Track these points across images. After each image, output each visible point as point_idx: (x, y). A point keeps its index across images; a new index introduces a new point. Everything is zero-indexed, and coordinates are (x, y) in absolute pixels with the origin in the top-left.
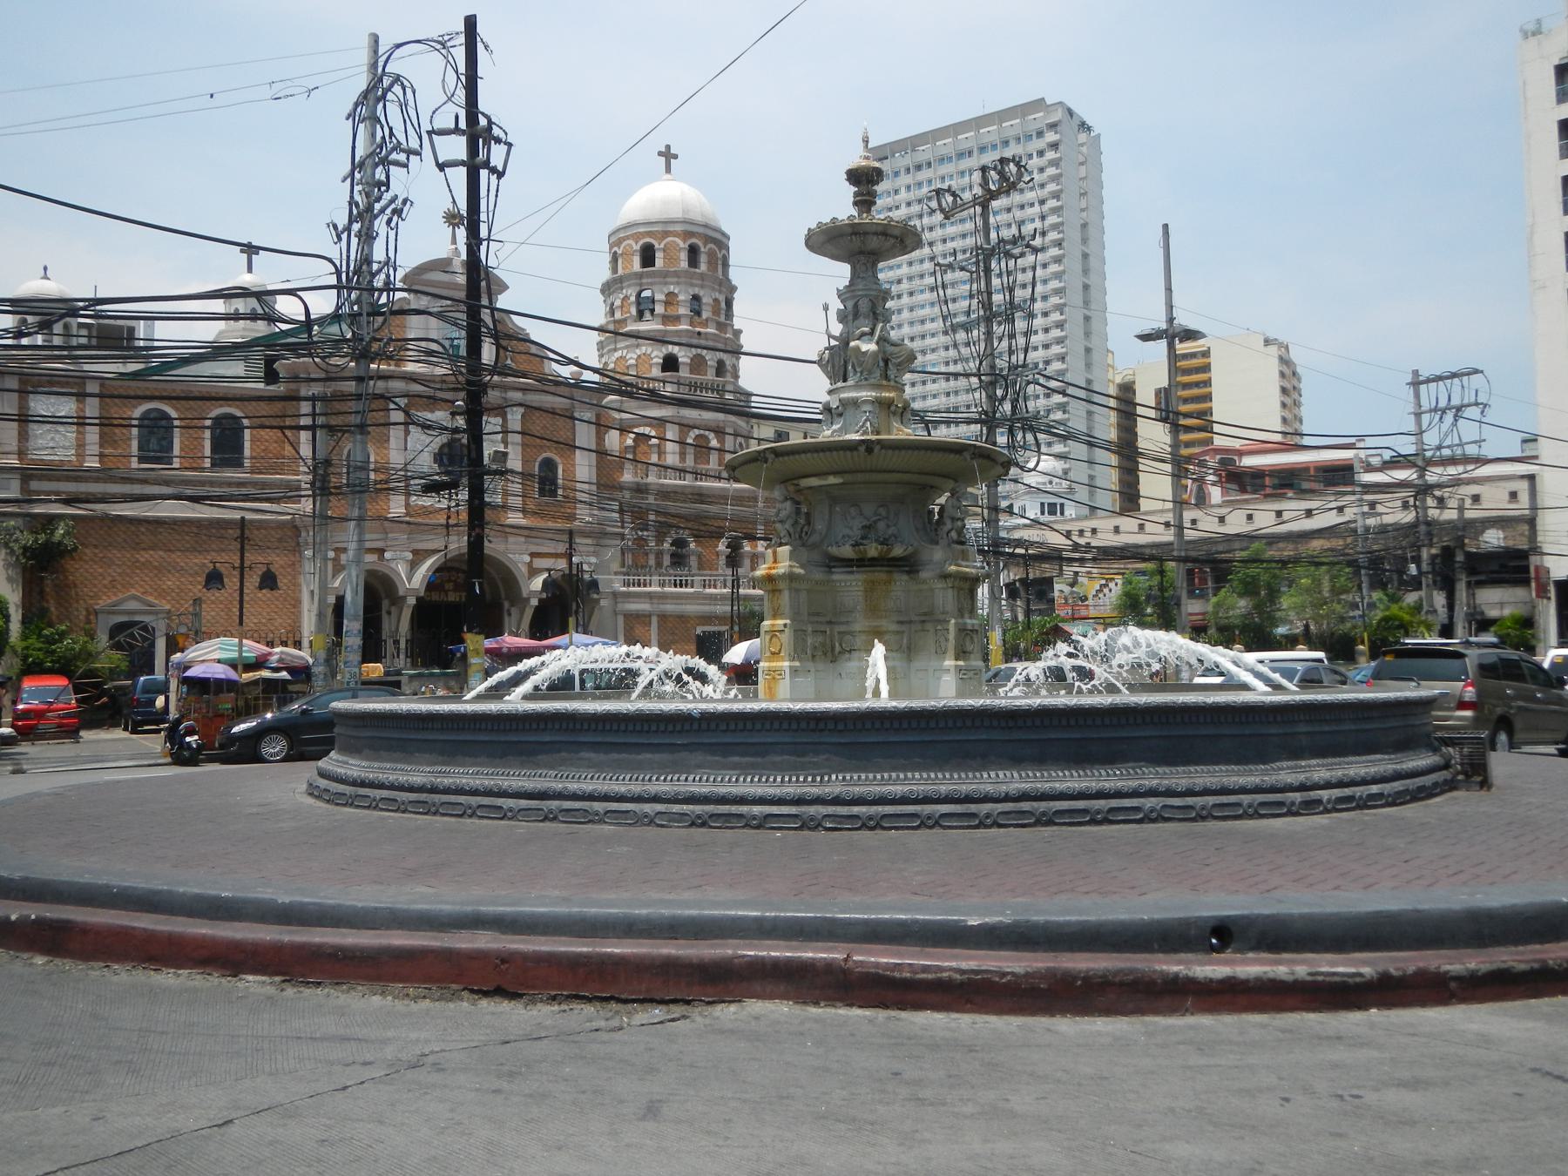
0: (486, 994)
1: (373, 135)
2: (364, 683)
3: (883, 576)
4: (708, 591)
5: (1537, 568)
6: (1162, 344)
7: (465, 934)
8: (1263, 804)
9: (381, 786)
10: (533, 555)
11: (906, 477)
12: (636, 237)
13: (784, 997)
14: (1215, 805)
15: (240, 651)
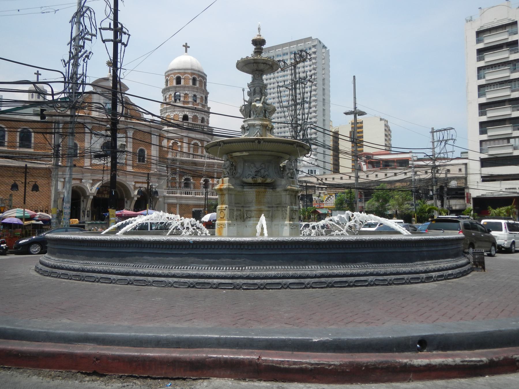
0: (89, 375)
1: (79, 29)
2: (71, 226)
3: (263, 190)
4: (197, 196)
5: (467, 193)
7: (80, 345)
8: (412, 279)
9: (62, 268)
10: (135, 182)
11: (273, 153)
12: (174, 74)
13: (229, 377)
14: (395, 279)
15: (24, 213)
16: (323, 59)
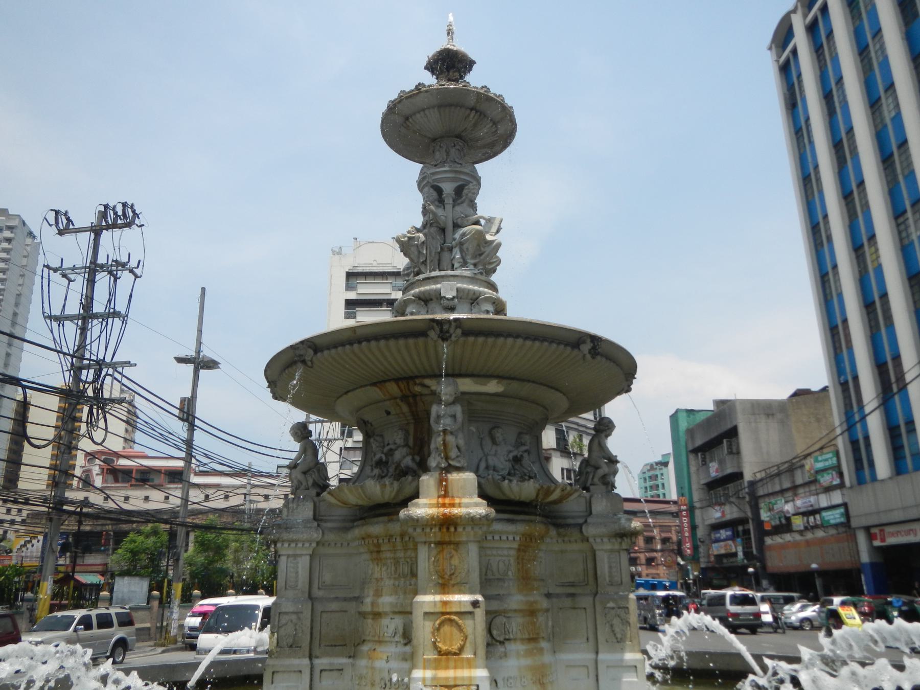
6: (190, 367)
16: (25, 257)
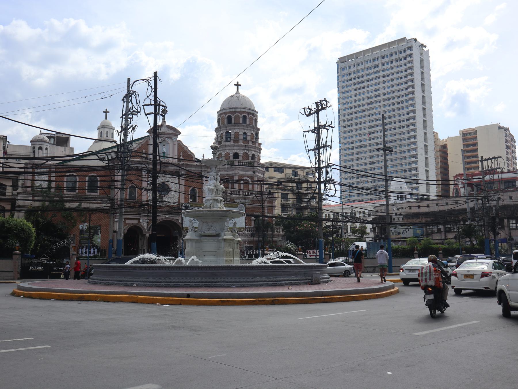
12: (226, 113)
